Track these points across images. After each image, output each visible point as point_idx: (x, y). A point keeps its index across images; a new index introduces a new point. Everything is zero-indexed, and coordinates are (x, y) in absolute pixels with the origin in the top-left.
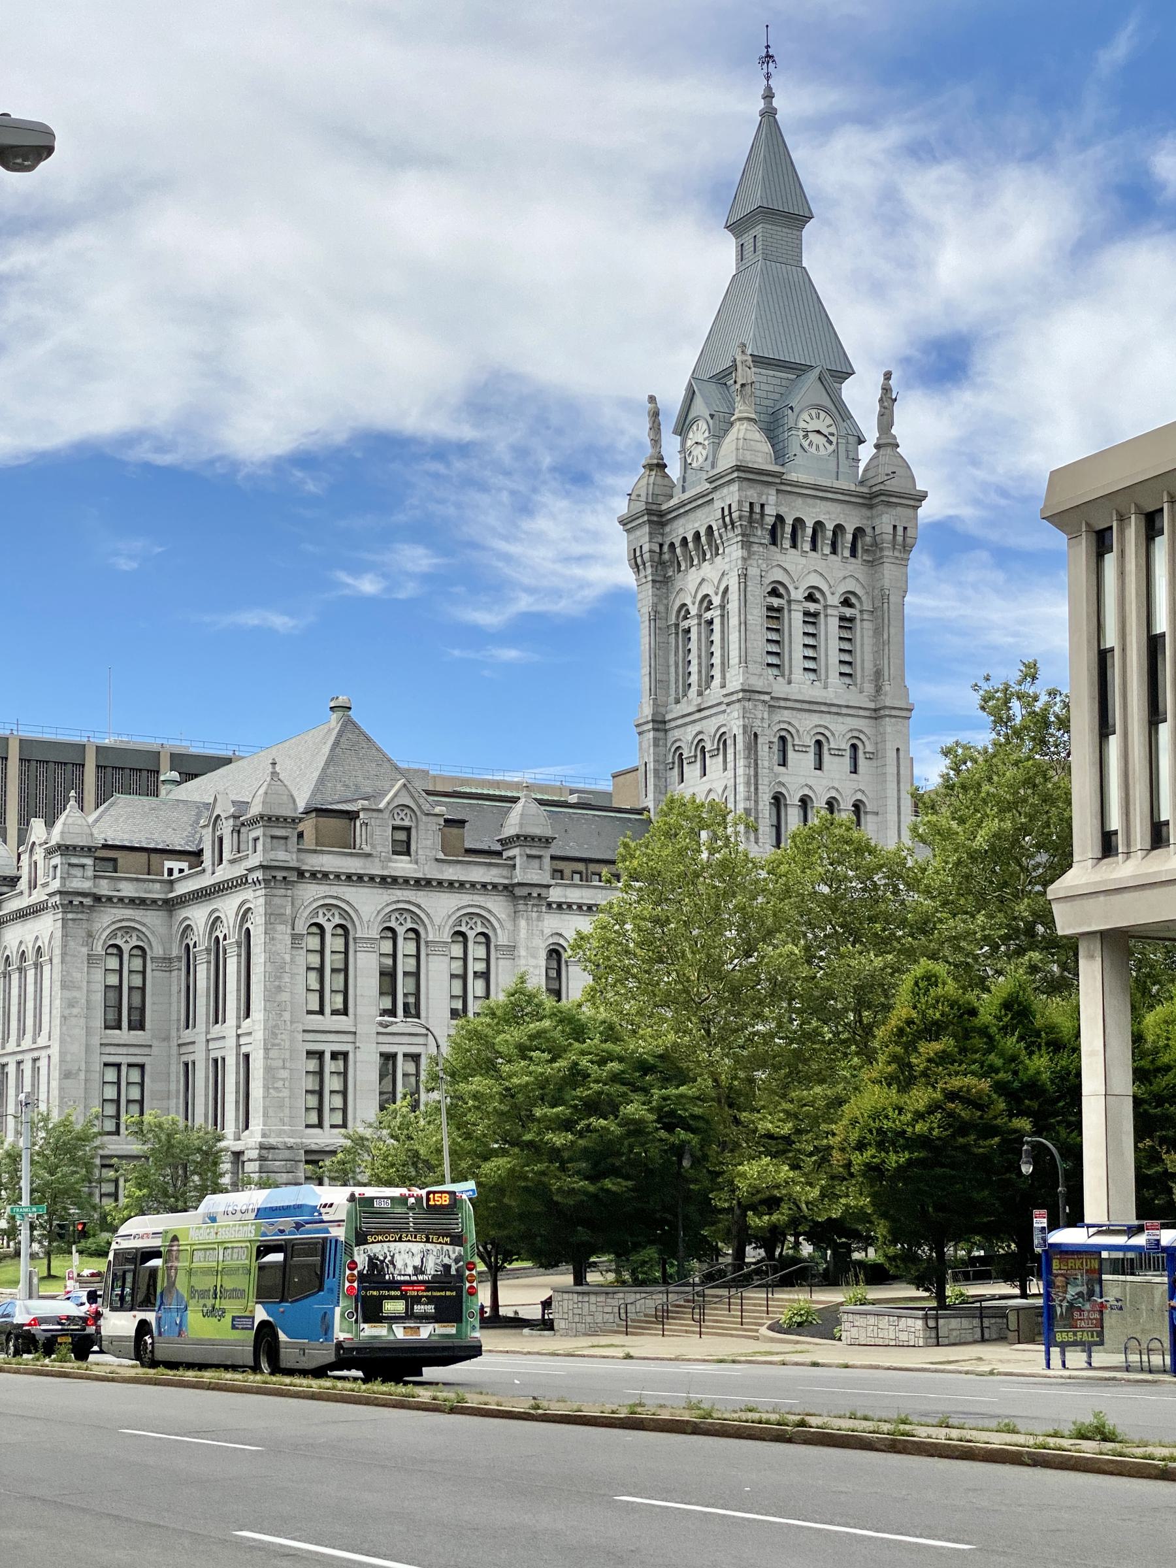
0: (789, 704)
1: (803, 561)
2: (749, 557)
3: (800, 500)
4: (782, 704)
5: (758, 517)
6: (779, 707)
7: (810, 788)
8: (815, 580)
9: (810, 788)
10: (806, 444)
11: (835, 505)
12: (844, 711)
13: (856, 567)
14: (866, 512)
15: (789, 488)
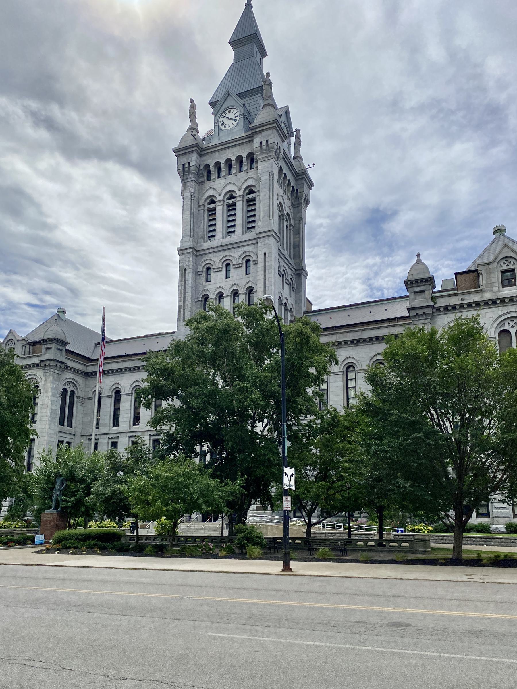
0: (211, 251)
1: (224, 181)
2: (185, 189)
3: (217, 153)
4: (207, 251)
5: (187, 169)
6: (206, 254)
7: (222, 288)
8: (229, 188)
9: (222, 288)
10: (222, 127)
11: (237, 147)
12: (241, 244)
13: (251, 173)
14: (249, 145)
15: (210, 151)
